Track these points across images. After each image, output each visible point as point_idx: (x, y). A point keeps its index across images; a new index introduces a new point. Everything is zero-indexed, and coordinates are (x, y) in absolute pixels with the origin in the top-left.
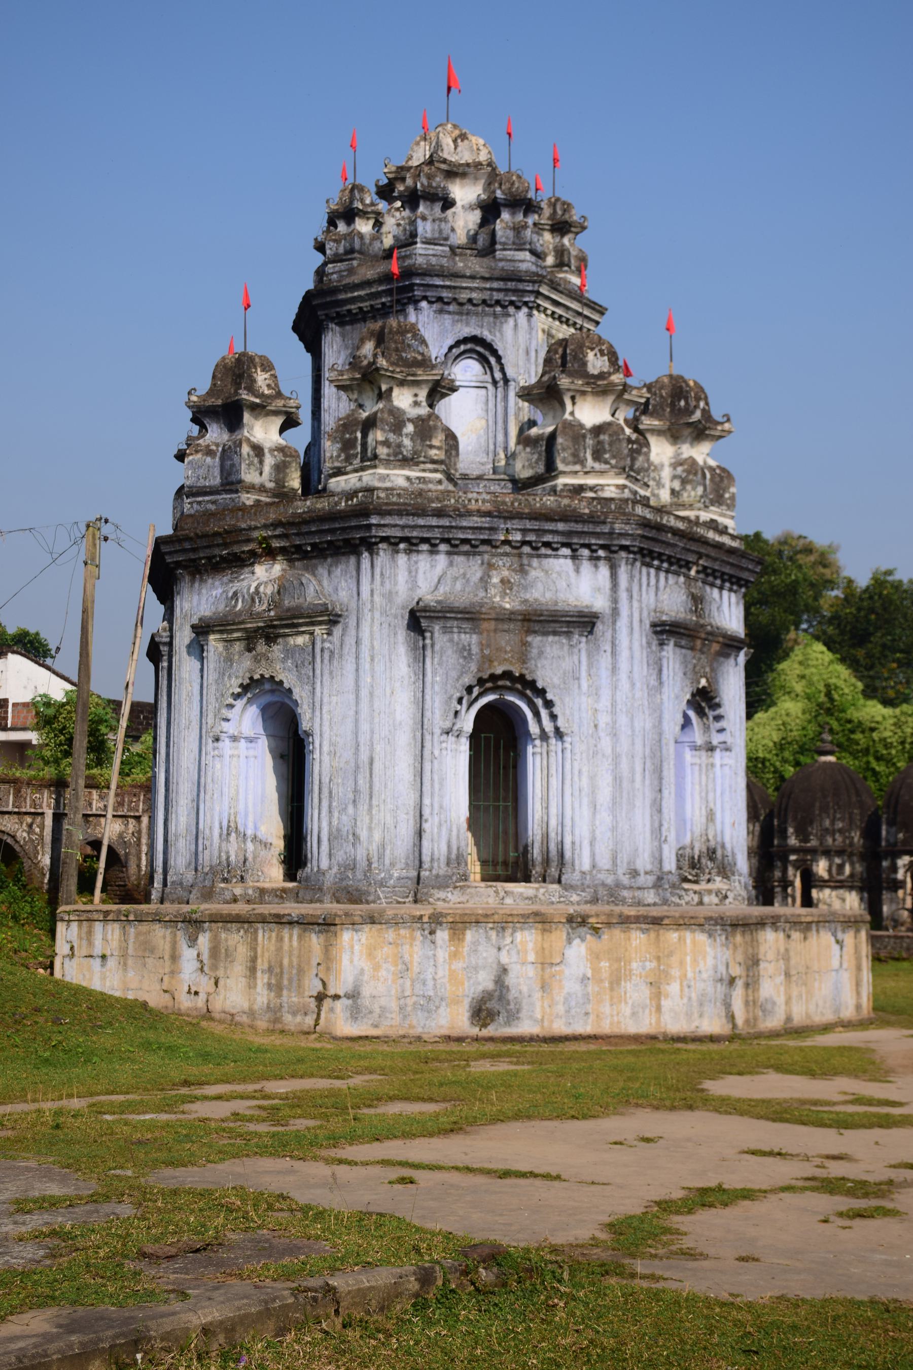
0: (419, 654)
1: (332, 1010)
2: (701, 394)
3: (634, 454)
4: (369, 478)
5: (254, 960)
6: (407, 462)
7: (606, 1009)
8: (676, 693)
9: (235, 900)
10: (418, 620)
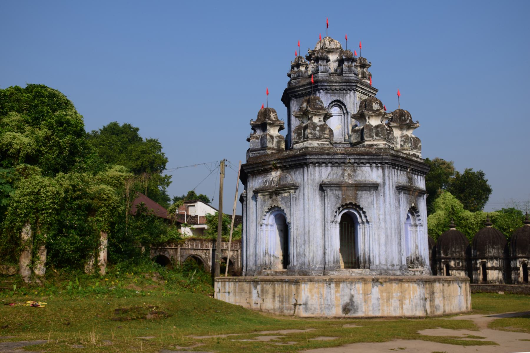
0: (323, 198)
1: (299, 309)
2: (409, 115)
3: (388, 134)
4: (306, 144)
5: (274, 293)
6: (317, 139)
7: (385, 308)
8: (404, 208)
9: (268, 275)
10: (323, 187)
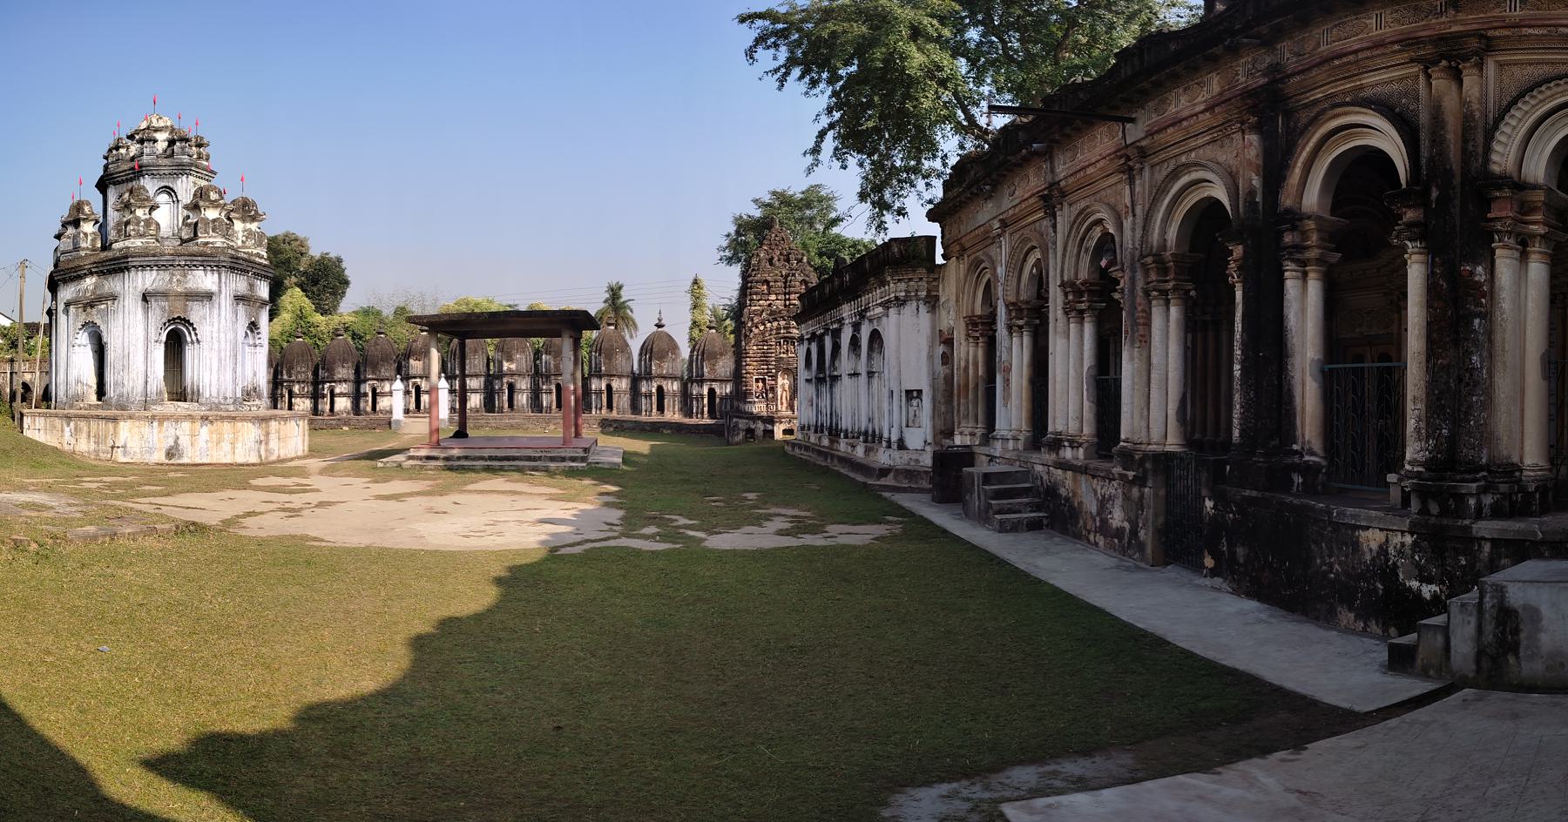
4: (127, 243)
6: (141, 236)
